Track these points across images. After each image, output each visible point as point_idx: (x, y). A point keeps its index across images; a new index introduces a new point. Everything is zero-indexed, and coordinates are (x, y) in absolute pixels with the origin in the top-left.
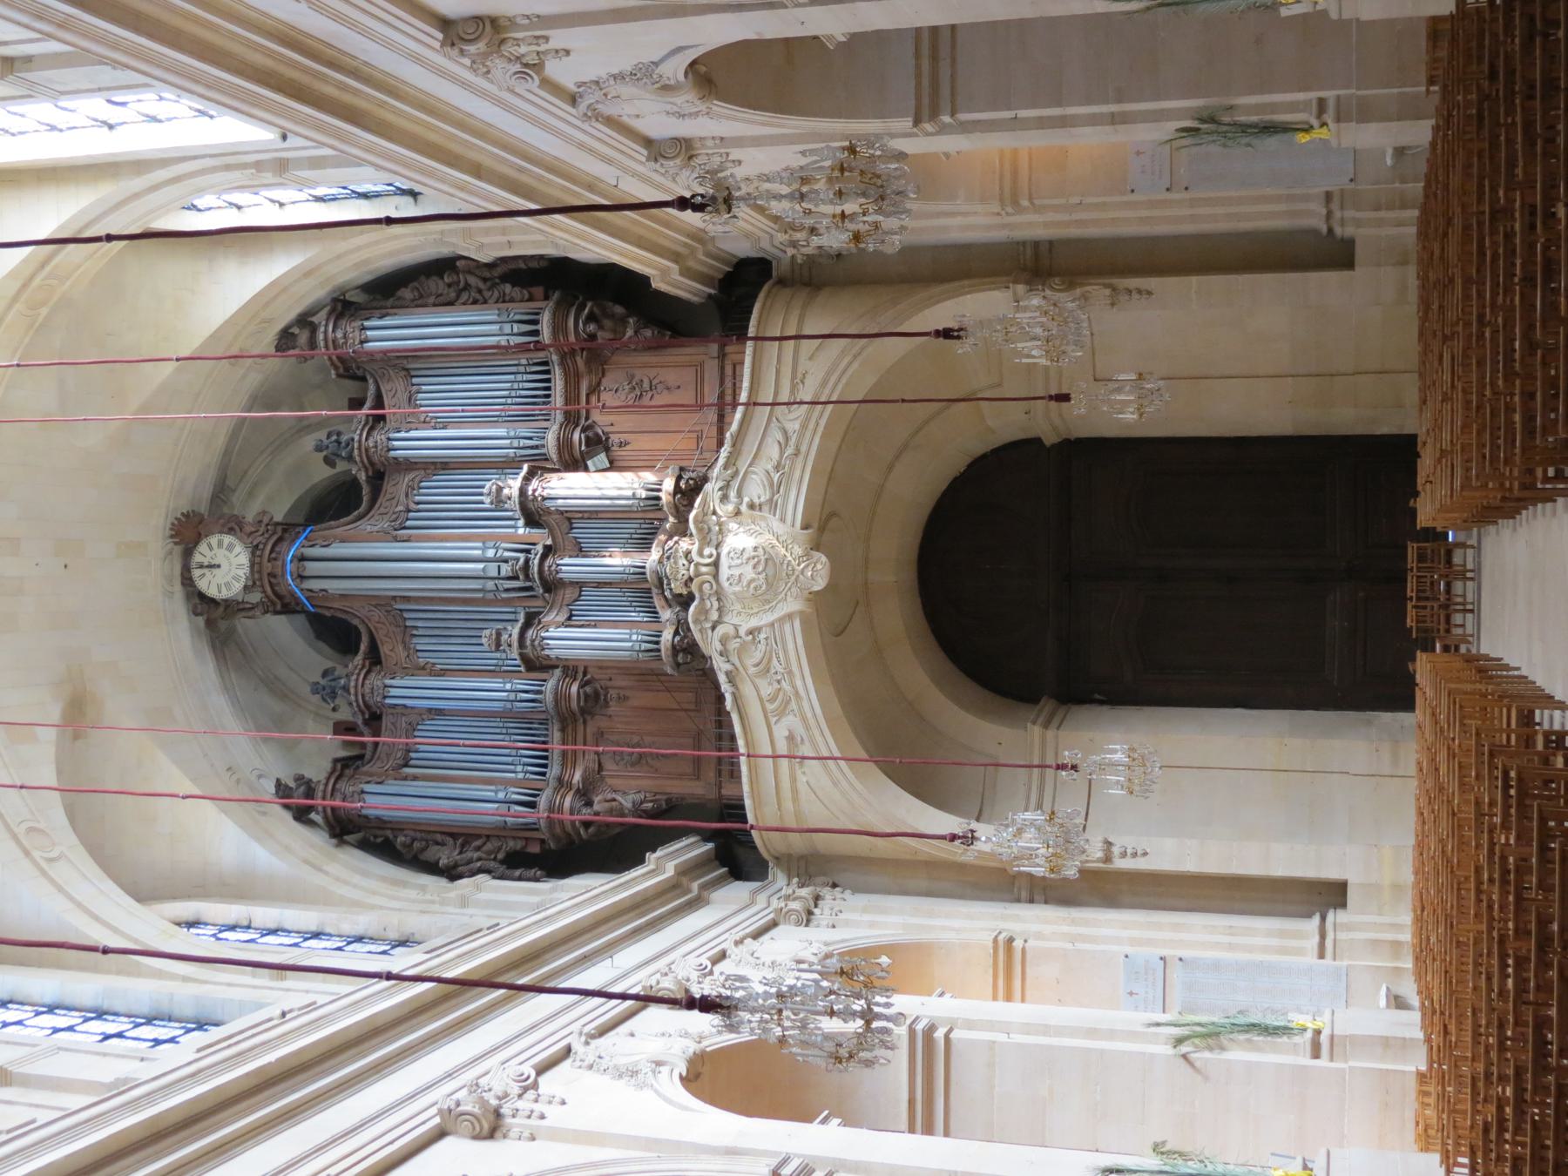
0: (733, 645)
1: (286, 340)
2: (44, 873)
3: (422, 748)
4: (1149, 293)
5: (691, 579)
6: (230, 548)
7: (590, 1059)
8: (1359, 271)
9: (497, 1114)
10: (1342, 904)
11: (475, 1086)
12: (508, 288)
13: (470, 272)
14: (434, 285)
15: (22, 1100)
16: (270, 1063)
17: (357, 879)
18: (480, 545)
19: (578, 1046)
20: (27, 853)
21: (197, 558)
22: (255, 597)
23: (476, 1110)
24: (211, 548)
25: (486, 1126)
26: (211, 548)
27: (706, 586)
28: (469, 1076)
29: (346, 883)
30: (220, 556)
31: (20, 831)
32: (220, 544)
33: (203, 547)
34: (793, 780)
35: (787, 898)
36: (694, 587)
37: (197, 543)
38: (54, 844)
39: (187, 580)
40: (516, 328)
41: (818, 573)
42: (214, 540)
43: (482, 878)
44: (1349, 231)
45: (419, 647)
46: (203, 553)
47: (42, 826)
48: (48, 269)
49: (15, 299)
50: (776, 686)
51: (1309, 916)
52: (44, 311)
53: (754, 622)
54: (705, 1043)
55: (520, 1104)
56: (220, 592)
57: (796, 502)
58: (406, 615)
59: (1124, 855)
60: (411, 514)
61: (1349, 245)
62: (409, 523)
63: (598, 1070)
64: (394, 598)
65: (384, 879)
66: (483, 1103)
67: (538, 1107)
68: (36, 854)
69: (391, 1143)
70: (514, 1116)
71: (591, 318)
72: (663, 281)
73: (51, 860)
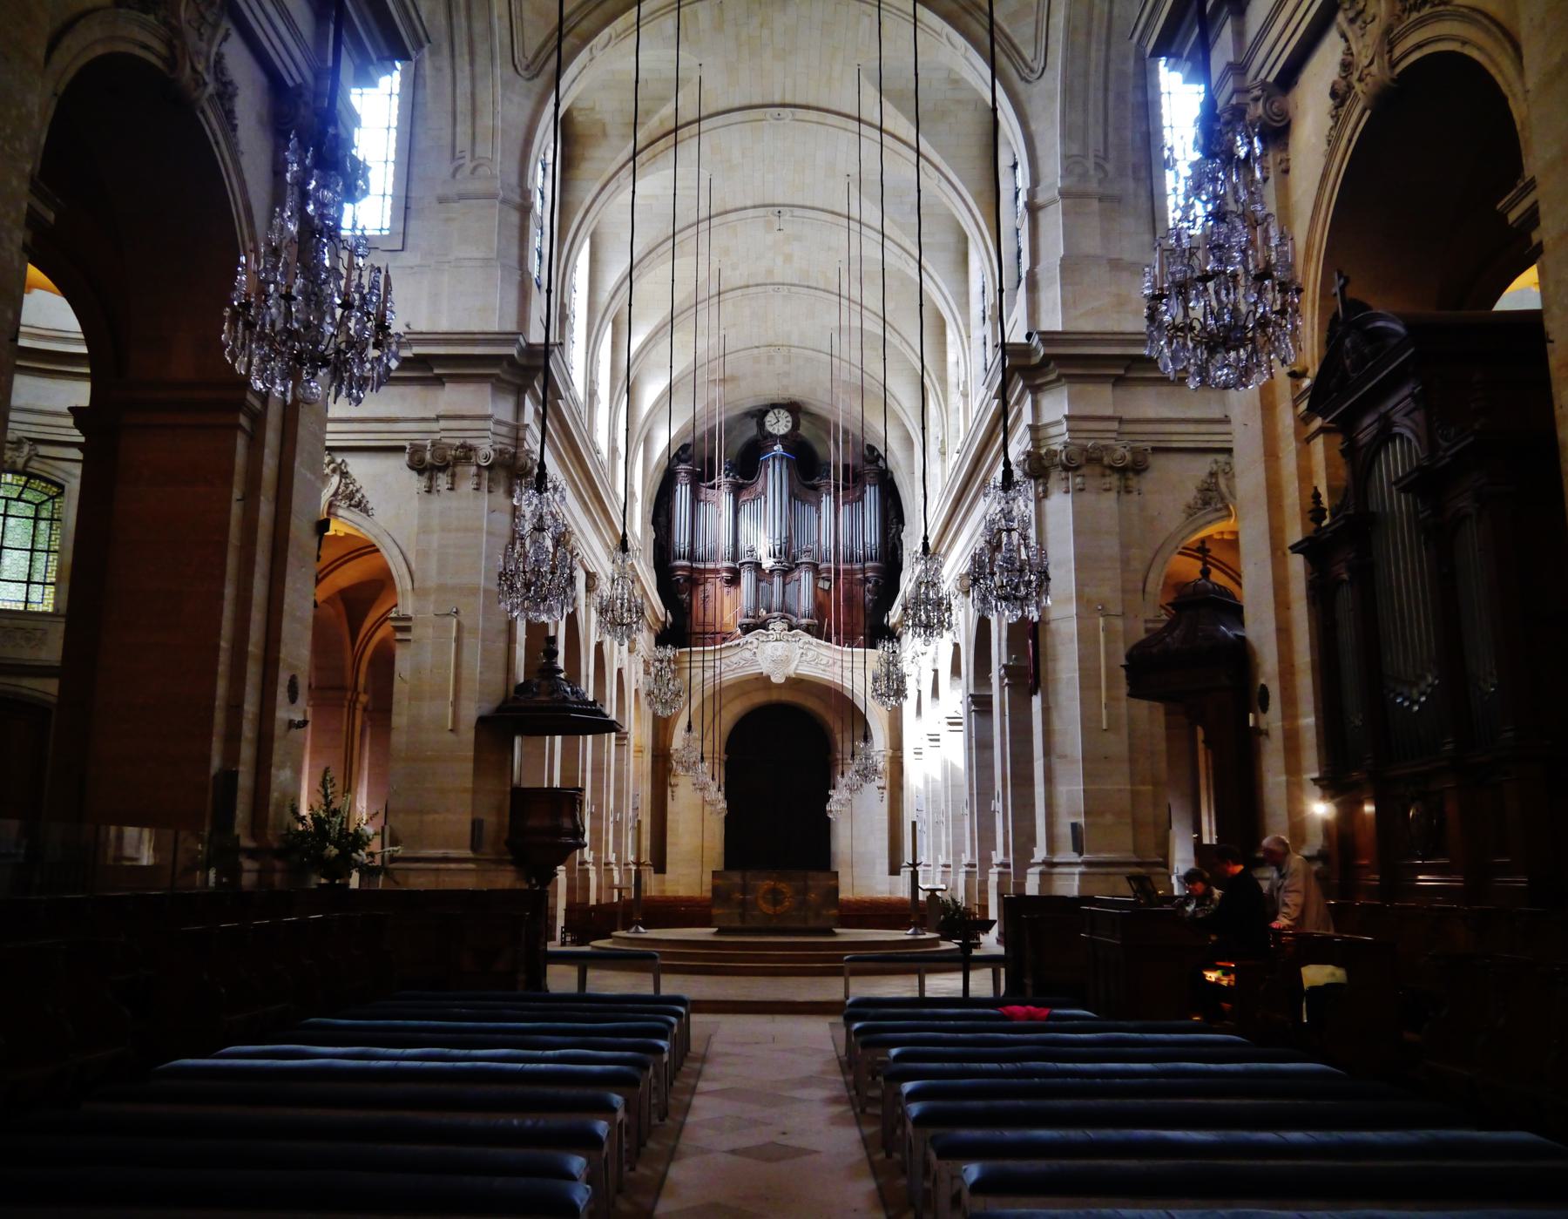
0: (749, 646)
1: (872, 449)
6: (786, 426)
10: (656, 872)
12: (890, 545)
13: (897, 528)
14: (892, 514)
21: (782, 411)
30: (783, 422)
33: (786, 414)
37: (788, 411)
39: (774, 406)
41: (778, 679)
42: (790, 419)
57: (807, 670)
59: (673, 792)
61: (897, 873)
71: (877, 582)
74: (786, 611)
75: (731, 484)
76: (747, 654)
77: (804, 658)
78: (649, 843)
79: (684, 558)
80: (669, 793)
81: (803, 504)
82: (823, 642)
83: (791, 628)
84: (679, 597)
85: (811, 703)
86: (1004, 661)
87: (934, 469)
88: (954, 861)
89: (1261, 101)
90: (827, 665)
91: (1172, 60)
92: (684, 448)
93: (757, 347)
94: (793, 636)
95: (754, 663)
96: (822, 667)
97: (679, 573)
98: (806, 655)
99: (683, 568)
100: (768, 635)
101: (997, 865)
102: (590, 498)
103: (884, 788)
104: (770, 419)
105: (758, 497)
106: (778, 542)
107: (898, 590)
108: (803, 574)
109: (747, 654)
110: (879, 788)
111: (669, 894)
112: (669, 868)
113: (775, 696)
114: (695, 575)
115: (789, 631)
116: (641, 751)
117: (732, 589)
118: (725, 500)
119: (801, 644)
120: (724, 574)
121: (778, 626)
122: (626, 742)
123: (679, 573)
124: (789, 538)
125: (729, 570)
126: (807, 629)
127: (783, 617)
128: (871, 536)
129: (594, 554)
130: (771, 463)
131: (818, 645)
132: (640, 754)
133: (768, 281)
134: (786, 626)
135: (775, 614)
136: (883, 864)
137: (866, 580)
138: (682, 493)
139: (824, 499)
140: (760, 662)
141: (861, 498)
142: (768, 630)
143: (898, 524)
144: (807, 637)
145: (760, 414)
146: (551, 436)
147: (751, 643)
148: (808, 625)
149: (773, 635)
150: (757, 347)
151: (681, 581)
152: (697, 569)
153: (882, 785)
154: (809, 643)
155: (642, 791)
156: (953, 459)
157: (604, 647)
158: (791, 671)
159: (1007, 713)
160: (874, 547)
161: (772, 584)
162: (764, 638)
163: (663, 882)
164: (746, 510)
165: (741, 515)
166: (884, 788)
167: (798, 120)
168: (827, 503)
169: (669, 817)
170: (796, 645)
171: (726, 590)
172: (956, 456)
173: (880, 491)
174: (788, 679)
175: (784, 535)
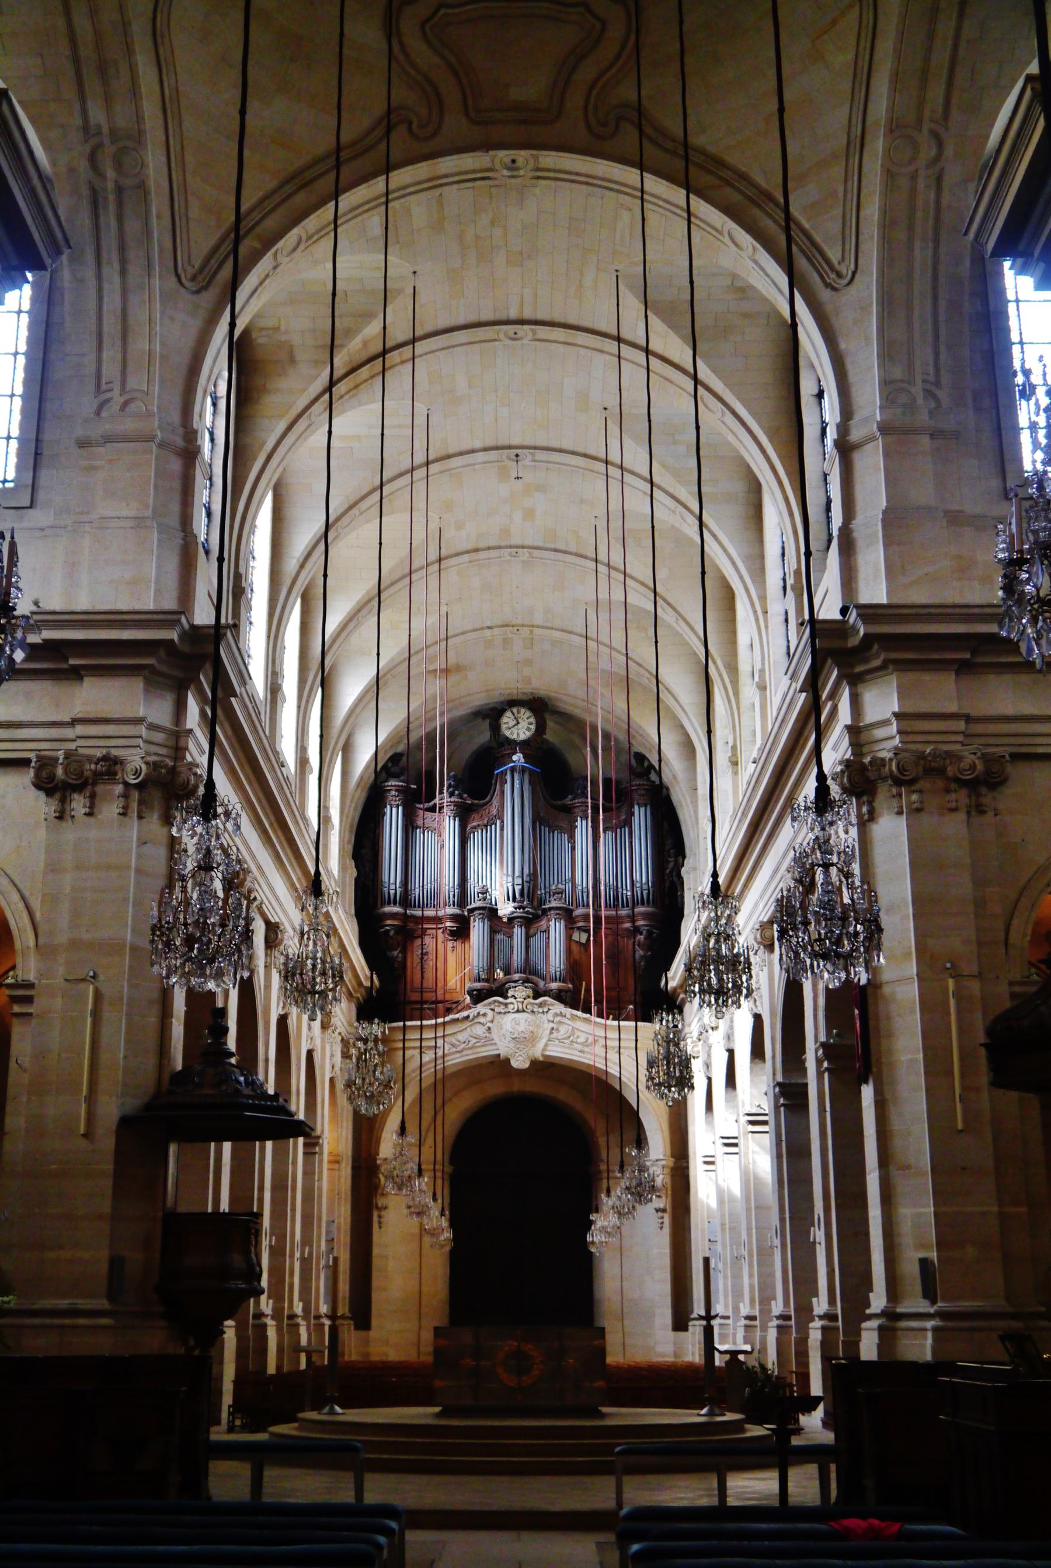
0: (482, 1020)
1: (640, 758)
4: (661, 1228)
5: (516, 998)
6: (528, 729)
8: (671, 1334)
10: (357, 1328)
12: (667, 884)
13: (676, 861)
14: (669, 842)
17: (353, 805)
18: (532, 871)
21: (523, 710)
24: (528, 718)
26: (528, 718)
29: (351, 802)
30: (524, 724)
33: (528, 714)
36: (510, 1000)
37: (531, 709)
39: (512, 703)
40: (645, 892)
41: (520, 1062)
42: (532, 720)
44: (690, 1328)
46: (525, 714)
50: (462, 1041)
51: (350, 1311)
57: (558, 1051)
58: (493, 826)
59: (380, 1217)
60: (547, 829)
64: (503, 822)
65: (353, 820)
71: (649, 933)
74: (531, 973)
75: (456, 804)
77: (555, 1035)
78: (347, 1287)
79: (395, 903)
80: (375, 1219)
81: (552, 830)
82: (579, 1013)
83: (537, 995)
84: (389, 954)
85: (564, 1095)
86: (822, 1038)
87: (724, 782)
88: (761, 1311)
90: (585, 1044)
91: (1020, 261)
92: (395, 758)
93: (489, 628)
94: (540, 1005)
95: (489, 1041)
96: (579, 1047)
97: (389, 922)
98: (557, 1030)
99: (393, 916)
100: (506, 1005)
101: (821, 1317)
102: (271, 825)
103: (664, 1210)
104: (507, 719)
106: (519, 881)
107: (677, 943)
108: (552, 923)
109: (479, 1030)
110: (657, 1210)
111: (374, 1358)
112: (374, 1322)
113: (517, 1086)
114: (411, 925)
115: (535, 998)
116: (338, 1162)
117: (458, 944)
118: (449, 826)
119: (550, 1016)
120: (448, 924)
121: (519, 993)
122: (317, 1149)
123: (389, 922)
124: (533, 876)
125: (454, 918)
126: (559, 997)
127: (526, 981)
128: (642, 872)
129: (277, 899)
130: (508, 777)
131: (574, 1018)
132: (336, 1166)
133: (503, 544)
134: (530, 992)
135: (516, 976)
136: (665, 1315)
138: (393, 818)
139: (579, 824)
140: (497, 1040)
141: (628, 823)
142: (506, 997)
143: (676, 856)
144: (559, 1007)
145: (493, 714)
146: (221, 745)
147: (484, 1015)
148: (560, 991)
149: (514, 1004)
150: (489, 628)
151: (392, 933)
152: (413, 917)
153: (662, 1206)
154: (561, 1015)
155: (339, 1217)
156: (748, 770)
157: (289, 1021)
158: (537, 1052)
159: (828, 1108)
160: (645, 887)
161: (511, 937)
162: (501, 1009)
163: (366, 1342)
164: (476, 839)
165: (470, 845)
166: (664, 1210)
168: (583, 830)
169: (376, 1251)
170: (544, 1017)
171: (450, 944)
173: (652, 813)
174: (534, 1063)
175: (526, 871)
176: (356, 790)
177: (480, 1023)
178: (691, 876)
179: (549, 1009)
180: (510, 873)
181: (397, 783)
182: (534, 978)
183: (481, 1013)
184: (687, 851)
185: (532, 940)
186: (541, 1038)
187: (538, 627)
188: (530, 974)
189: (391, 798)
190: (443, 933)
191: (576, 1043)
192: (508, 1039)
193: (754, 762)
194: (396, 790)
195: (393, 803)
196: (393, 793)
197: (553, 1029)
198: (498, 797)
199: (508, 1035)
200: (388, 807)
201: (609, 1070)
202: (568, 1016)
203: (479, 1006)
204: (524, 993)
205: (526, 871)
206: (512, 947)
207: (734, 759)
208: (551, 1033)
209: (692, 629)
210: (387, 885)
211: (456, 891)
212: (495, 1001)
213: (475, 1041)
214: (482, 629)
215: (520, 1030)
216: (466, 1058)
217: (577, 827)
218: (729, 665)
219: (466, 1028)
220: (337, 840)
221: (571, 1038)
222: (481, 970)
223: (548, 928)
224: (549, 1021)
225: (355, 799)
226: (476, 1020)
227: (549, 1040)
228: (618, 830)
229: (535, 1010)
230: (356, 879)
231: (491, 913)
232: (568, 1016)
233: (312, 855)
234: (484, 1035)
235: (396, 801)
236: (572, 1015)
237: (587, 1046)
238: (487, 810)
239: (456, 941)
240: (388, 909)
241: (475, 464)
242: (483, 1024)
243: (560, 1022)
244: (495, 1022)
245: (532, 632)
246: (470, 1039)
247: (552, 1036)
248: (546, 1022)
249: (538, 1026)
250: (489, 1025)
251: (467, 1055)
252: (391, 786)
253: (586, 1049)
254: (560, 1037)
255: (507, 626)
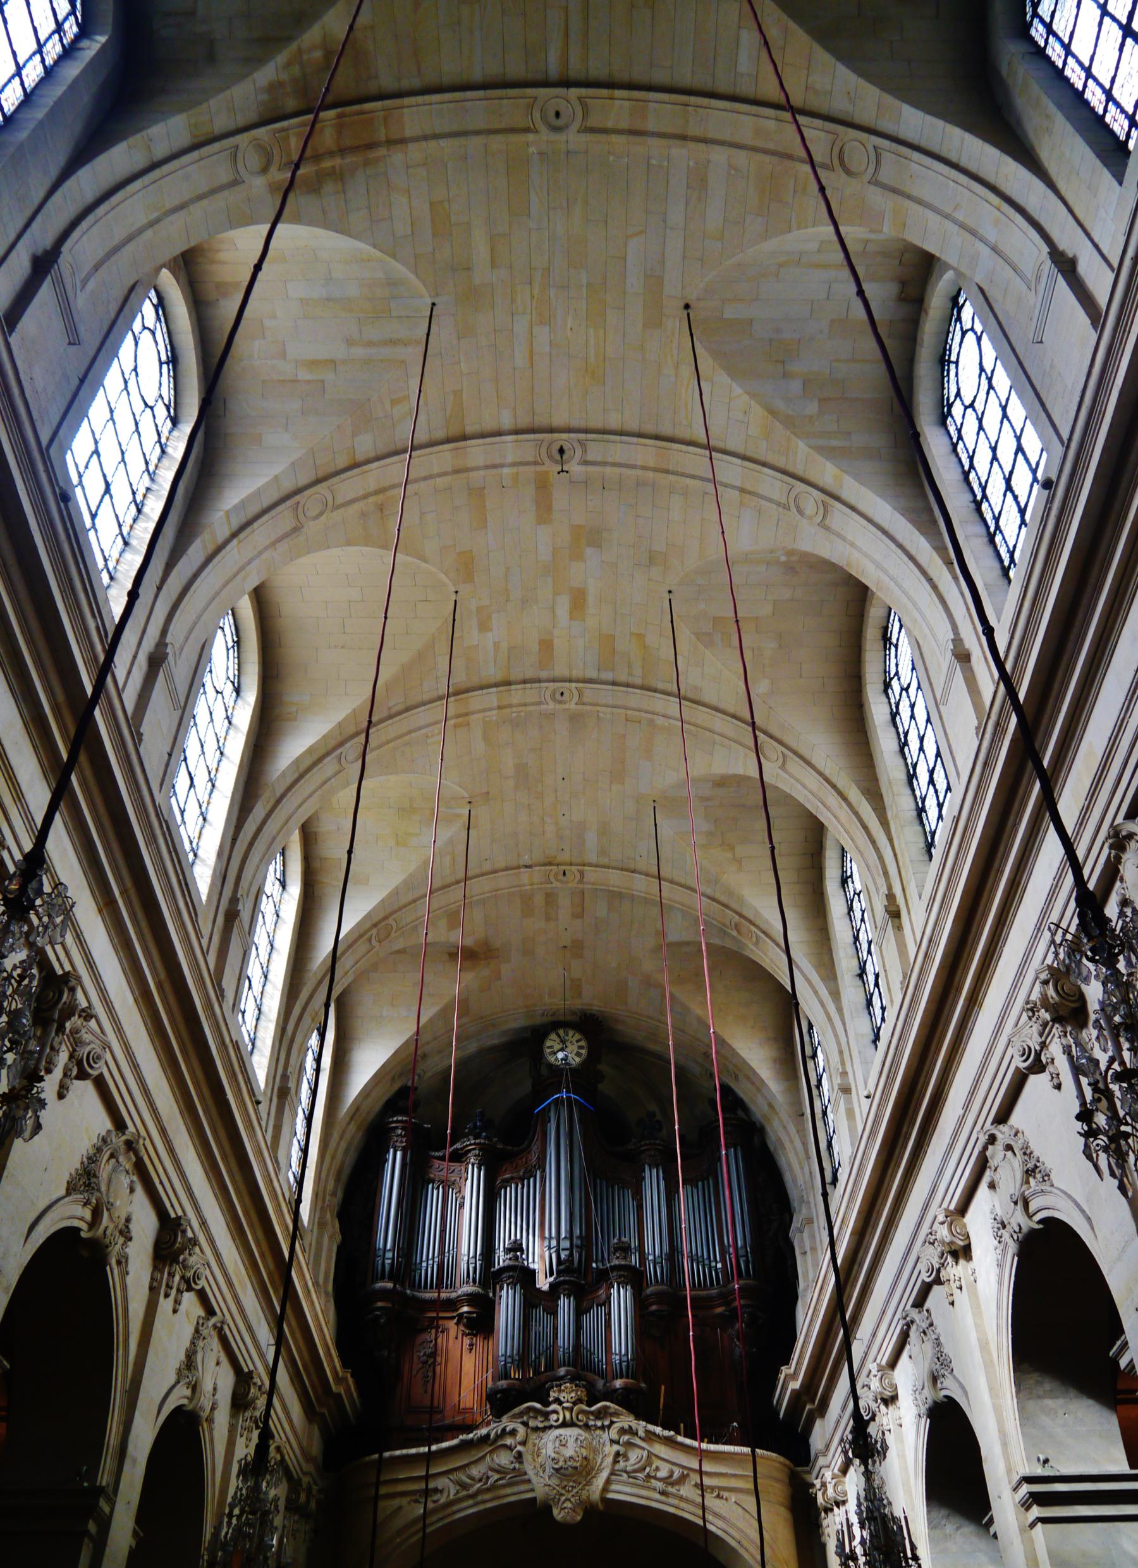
0: (509, 1441)
2: (361, 936)
3: (435, 1192)
5: (560, 1403)
7: (205, 1332)
9: (174, 1260)
11: (194, 1242)
15: (215, 929)
16: (226, 1095)
17: (343, 1145)
19: (213, 1320)
20: (375, 925)
21: (571, 1033)
22: (544, 1071)
23: (177, 1245)
24: (577, 1041)
25: (165, 1252)
26: (577, 1041)
27: (554, 1417)
28: (202, 1239)
29: (341, 1138)
30: (572, 1048)
31: (391, 921)
32: (581, 1047)
33: (578, 1036)
34: (403, 1494)
35: (309, 1491)
38: (380, 942)
39: (555, 1025)
42: (582, 1043)
43: (339, 1238)
45: (508, 1189)
46: (573, 1036)
47: (393, 935)
48: (762, 935)
49: (741, 916)
50: (477, 1477)
52: (734, 933)
53: (527, 1458)
54: (205, 1425)
55: (177, 1278)
56: (548, 1048)
57: (623, 1492)
62: (598, 1181)
63: (194, 1338)
65: (342, 1166)
66: (181, 1251)
67: (174, 1292)
68: (374, 931)
69: (161, 1183)
70: (169, 1274)
72: (786, 1376)
73: (370, 940)
76: (504, 1459)
77: (622, 1465)
82: (658, 1430)
87: (837, 1118)
89: (1051, 983)
92: (403, 1093)
93: (526, 867)
94: (599, 1415)
95: (518, 1476)
96: (659, 1485)
97: (380, 1304)
99: (384, 1294)
100: (546, 1415)
104: (552, 1042)
105: (530, 1174)
106: (565, 1244)
108: (614, 1291)
109: (504, 1459)
115: (590, 1405)
117: (479, 1341)
119: (613, 1433)
120: (465, 1309)
121: (567, 1394)
123: (380, 1304)
125: (471, 1299)
128: (738, 1235)
130: (552, 1114)
131: (650, 1437)
133: (544, 674)
134: (582, 1393)
137: (731, 1317)
140: (531, 1474)
144: (626, 1420)
149: (559, 1414)
150: (526, 867)
152: (414, 1298)
156: (862, 1107)
161: (554, 1312)
164: (509, 1194)
167: (592, 130)
170: (605, 1436)
171: (467, 1341)
172: (866, 1103)
174: (590, 1510)
175: (577, 1232)
176: (349, 1123)
177: (505, 1446)
178: (806, 1235)
179: (612, 1423)
180: (553, 1234)
181: (404, 1118)
182: (591, 1375)
183: (508, 1429)
184: (795, 1204)
185: (585, 1319)
186: (600, 1470)
187: (590, 865)
188: (583, 1368)
189: (395, 1138)
190: (457, 1324)
191: (655, 1478)
192: (549, 1471)
193: (868, 1097)
194: (403, 1129)
195: (398, 1144)
196: (399, 1131)
197: (618, 1454)
198: (539, 1143)
199: (549, 1464)
200: (391, 1150)
201: (710, 1527)
202: (641, 1433)
203: (504, 1419)
204: (573, 1395)
205: (577, 1232)
206: (556, 1328)
207: (892, 909)
208: (615, 1461)
209: (778, 945)
210: (381, 1253)
211: (478, 1263)
212: (530, 1409)
213: (496, 1476)
214: (518, 867)
215: (568, 1455)
216: (482, 1507)
217: (644, 1178)
218: (868, 790)
219: (484, 1457)
220: (313, 1175)
221: (648, 1469)
222: (509, 1360)
223: (609, 1297)
224: (612, 1442)
225: (348, 1136)
226: (500, 1443)
227: (612, 1473)
228: (700, 1184)
229: (591, 1423)
230: (339, 1248)
231: (528, 1276)
232: (641, 1433)
233: (287, 1227)
234: (512, 1467)
235: (402, 1142)
236: (647, 1432)
237: (672, 1484)
238: (524, 1160)
239: (475, 1335)
240: (380, 1285)
241: (502, 466)
242: (510, 1448)
243: (629, 1444)
244: (530, 1444)
245: (582, 873)
246: (490, 1473)
247: (617, 1467)
248: (608, 1443)
249: (595, 1451)
250: (519, 1448)
251: (484, 1502)
252: (397, 1121)
253: (670, 1489)
254: (629, 1469)
255: (550, 864)
